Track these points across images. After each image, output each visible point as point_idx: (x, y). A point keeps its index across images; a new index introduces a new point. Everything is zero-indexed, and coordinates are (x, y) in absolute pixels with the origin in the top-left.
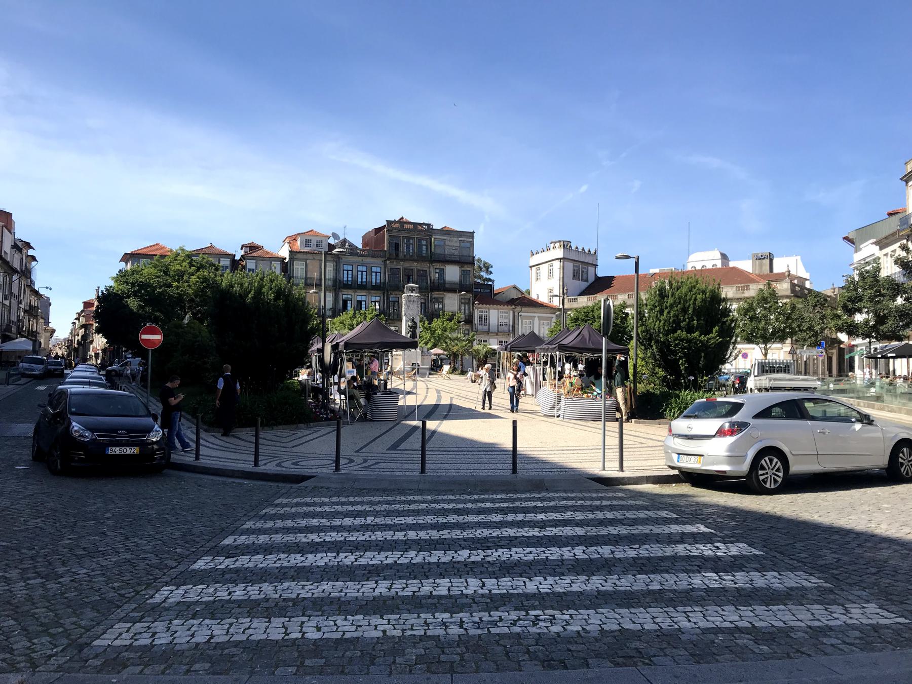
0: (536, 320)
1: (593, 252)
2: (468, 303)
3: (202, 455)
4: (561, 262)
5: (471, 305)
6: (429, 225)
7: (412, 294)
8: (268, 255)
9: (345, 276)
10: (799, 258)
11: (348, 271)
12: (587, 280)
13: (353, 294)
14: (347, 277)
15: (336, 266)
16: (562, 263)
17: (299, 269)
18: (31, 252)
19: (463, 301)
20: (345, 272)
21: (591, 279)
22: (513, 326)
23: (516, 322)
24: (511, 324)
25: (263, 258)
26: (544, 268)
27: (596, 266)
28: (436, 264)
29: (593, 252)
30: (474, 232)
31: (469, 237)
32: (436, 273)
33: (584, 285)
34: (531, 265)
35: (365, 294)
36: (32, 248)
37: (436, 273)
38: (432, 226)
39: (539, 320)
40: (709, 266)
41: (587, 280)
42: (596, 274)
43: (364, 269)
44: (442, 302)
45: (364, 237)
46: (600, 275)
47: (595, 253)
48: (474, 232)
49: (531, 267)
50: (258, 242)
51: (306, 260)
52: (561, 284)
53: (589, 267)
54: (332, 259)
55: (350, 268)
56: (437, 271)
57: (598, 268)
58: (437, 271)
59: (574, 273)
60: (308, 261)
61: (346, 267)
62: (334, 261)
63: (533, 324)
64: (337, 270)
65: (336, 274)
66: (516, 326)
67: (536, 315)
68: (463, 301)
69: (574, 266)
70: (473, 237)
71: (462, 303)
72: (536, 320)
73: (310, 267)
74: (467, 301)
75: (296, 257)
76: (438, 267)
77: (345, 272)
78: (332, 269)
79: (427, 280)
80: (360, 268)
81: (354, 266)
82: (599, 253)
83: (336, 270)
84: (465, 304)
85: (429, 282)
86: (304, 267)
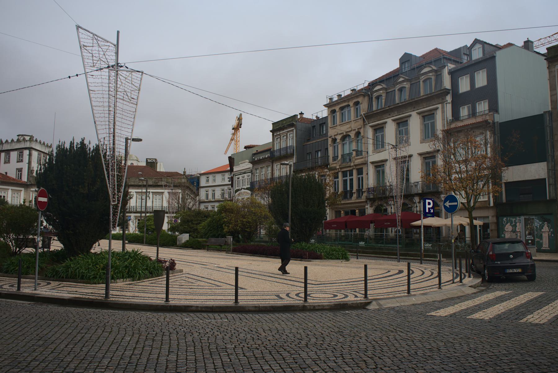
39: (12, 192)
67: (10, 188)
69: (38, 154)
72: (10, 192)
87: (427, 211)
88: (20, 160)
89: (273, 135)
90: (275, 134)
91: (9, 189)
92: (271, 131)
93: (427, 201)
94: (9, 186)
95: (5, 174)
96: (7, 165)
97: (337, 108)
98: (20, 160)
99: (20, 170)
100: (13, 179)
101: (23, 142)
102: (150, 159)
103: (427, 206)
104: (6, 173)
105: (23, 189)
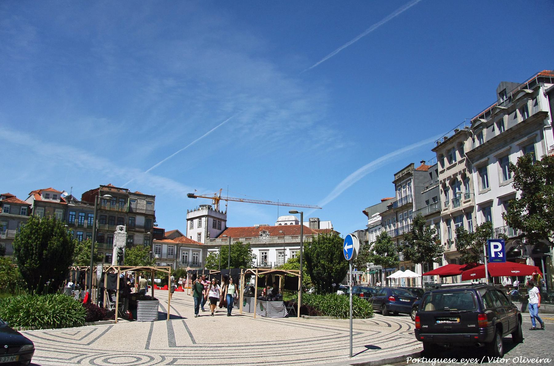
0: (191, 251)
1: (224, 212)
2: (149, 240)
3: (348, 331)
5: (151, 241)
7: (121, 232)
8: (20, 202)
9: (70, 218)
10: (330, 222)
11: (72, 215)
15: (65, 212)
19: (146, 238)
20: (71, 216)
22: (176, 255)
23: (178, 252)
24: (175, 253)
25: (16, 204)
26: (196, 221)
27: (225, 221)
28: (130, 214)
29: (224, 212)
32: (129, 220)
35: (82, 231)
37: (129, 220)
39: (192, 252)
40: (289, 223)
42: (225, 226)
43: (83, 214)
44: (133, 238)
45: (83, 195)
47: (226, 213)
50: (12, 193)
51: (45, 207)
52: (206, 230)
54: (62, 207)
55: (74, 213)
56: (130, 218)
58: (130, 218)
59: (213, 224)
60: (46, 208)
61: (71, 213)
65: (64, 216)
66: (178, 255)
67: (191, 249)
68: (146, 238)
69: (214, 220)
72: (191, 251)
74: (148, 238)
76: (131, 216)
77: (71, 216)
78: (62, 213)
80: (80, 214)
82: (228, 214)
83: (65, 214)
86: (43, 211)
87: (493, 255)
88: (200, 225)
89: (395, 185)
90: (397, 185)
92: (393, 183)
93: (492, 244)
94: (190, 247)
95: (190, 238)
96: (192, 230)
97: (443, 152)
98: (200, 225)
99: (200, 234)
100: (194, 242)
101: (202, 210)
102: (313, 219)
103: (493, 250)
104: (191, 237)
105: (201, 250)
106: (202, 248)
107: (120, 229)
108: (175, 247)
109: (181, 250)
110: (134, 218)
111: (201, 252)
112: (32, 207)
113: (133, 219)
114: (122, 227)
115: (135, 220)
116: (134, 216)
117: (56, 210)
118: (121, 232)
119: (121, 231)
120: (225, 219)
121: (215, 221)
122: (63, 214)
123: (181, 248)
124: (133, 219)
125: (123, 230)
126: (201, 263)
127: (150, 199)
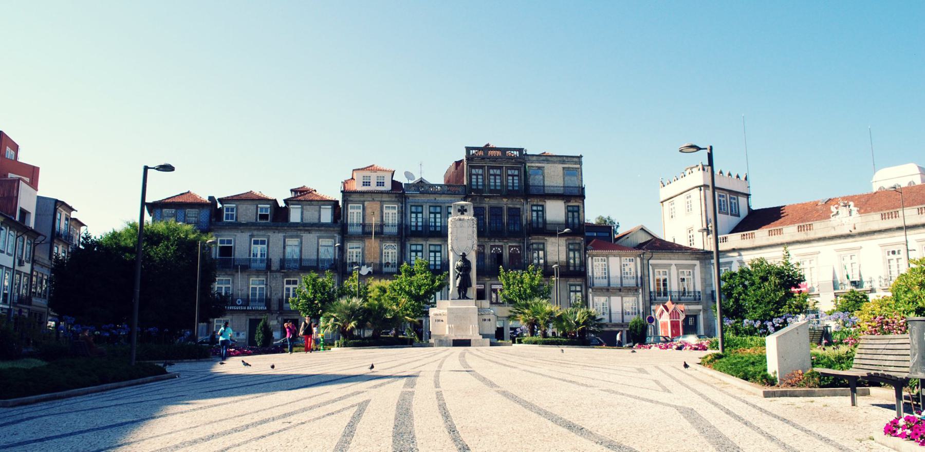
0: (673, 268)
2: (579, 251)
4: (701, 190)
5: (582, 251)
6: (520, 150)
12: (739, 215)
13: (424, 243)
14: (414, 220)
15: (402, 207)
16: (702, 192)
17: (355, 215)
18: (73, 215)
19: (571, 247)
21: (744, 212)
22: (641, 278)
23: (646, 272)
24: (639, 275)
25: (311, 202)
27: (747, 196)
28: (532, 199)
30: (581, 156)
31: (576, 163)
32: (533, 211)
33: (735, 221)
34: (662, 200)
36: (73, 210)
37: (533, 211)
38: (525, 151)
39: (678, 269)
41: (739, 215)
42: (749, 207)
44: (543, 250)
46: (754, 208)
47: (746, 179)
48: (581, 156)
49: (662, 202)
50: (309, 186)
53: (739, 198)
54: (396, 199)
56: (535, 208)
57: (752, 199)
58: (535, 208)
60: (366, 203)
62: (398, 201)
63: (670, 274)
64: (403, 214)
65: (402, 218)
67: (673, 262)
68: (571, 247)
70: (580, 163)
71: (570, 250)
72: (673, 268)
73: (368, 211)
74: (577, 247)
75: (351, 199)
76: (535, 203)
78: (396, 211)
79: (521, 220)
81: (424, 206)
83: (402, 213)
84: (574, 250)
85: (524, 222)
86: (361, 211)
91: (672, 264)
94: (670, 259)
105: (697, 263)
106: (698, 259)
107: (459, 211)
108: (636, 260)
109: (650, 267)
110: (542, 206)
111: (698, 269)
112: (340, 204)
113: (540, 208)
114: (462, 207)
115: (543, 211)
116: (540, 203)
117: (385, 206)
118: (462, 217)
119: (462, 214)
120: (745, 192)
121: (723, 196)
122: (398, 213)
123: (651, 262)
124: (540, 208)
125: (466, 211)
126: (699, 292)
127: (573, 163)
